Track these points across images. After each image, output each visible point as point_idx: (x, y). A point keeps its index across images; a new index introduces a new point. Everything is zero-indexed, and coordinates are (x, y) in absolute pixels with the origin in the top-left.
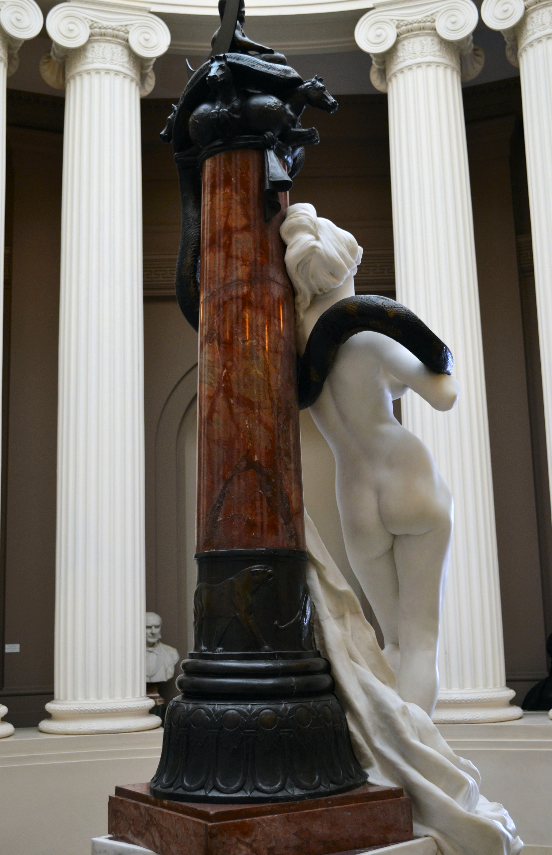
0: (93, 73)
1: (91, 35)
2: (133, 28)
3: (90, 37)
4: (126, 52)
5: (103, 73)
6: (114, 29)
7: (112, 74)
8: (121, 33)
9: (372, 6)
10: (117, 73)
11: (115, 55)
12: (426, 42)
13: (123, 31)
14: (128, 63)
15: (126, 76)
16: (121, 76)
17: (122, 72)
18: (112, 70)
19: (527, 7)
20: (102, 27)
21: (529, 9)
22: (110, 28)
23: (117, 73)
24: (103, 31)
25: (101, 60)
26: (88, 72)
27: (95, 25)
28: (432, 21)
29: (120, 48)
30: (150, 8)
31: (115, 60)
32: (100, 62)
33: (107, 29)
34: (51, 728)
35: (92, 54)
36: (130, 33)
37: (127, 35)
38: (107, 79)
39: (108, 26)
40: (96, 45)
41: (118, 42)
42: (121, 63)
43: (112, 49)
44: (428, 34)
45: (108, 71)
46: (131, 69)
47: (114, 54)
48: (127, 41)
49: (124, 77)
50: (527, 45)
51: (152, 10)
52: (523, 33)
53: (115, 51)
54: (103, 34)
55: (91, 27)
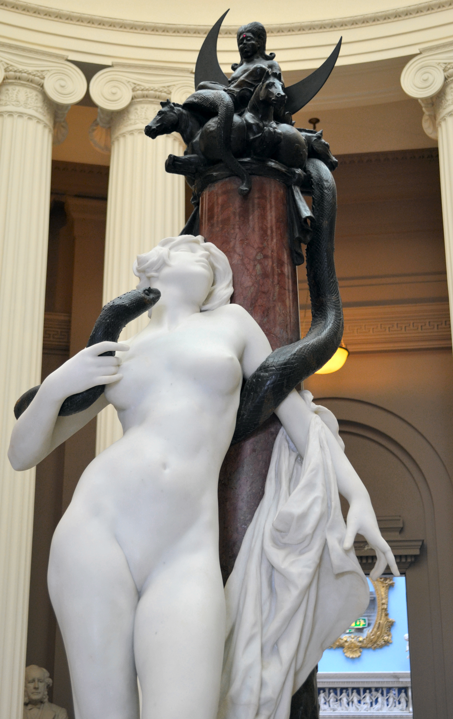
1: (6, 78)
2: (49, 74)
3: (4, 79)
4: (40, 97)
6: (29, 74)
7: (26, 118)
8: (37, 78)
10: (31, 117)
11: (30, 99)
14: (42, 108)
15: (39, 121)
16: (35, 121)
17: (35, 117)
18: (26, 114)
19: (447, 77)
20: (18, 71)
21: (449, 80)
22: (25, 72)
23: (31, 117)
24: (18, 74)
25: (14, 103)
29: (34, 93)
30: (68, 56)
31: (29, 104)
32: (13, 105)
33: (22, 73)
35: (6, 96)
36: (172, 94)
37: (42, 81)
38: (20, 122)
41: (33, 87)
42: (35, 108)
43: (26, 93)
45: (21, 115)
46: (45, 114)
47: (28, 98)
48: (42, 86)
49: (38, 122)
50: (446, 114)
51: (70, 58)
52: (442, 103)
53: (30, 95)
54: (18, 78)
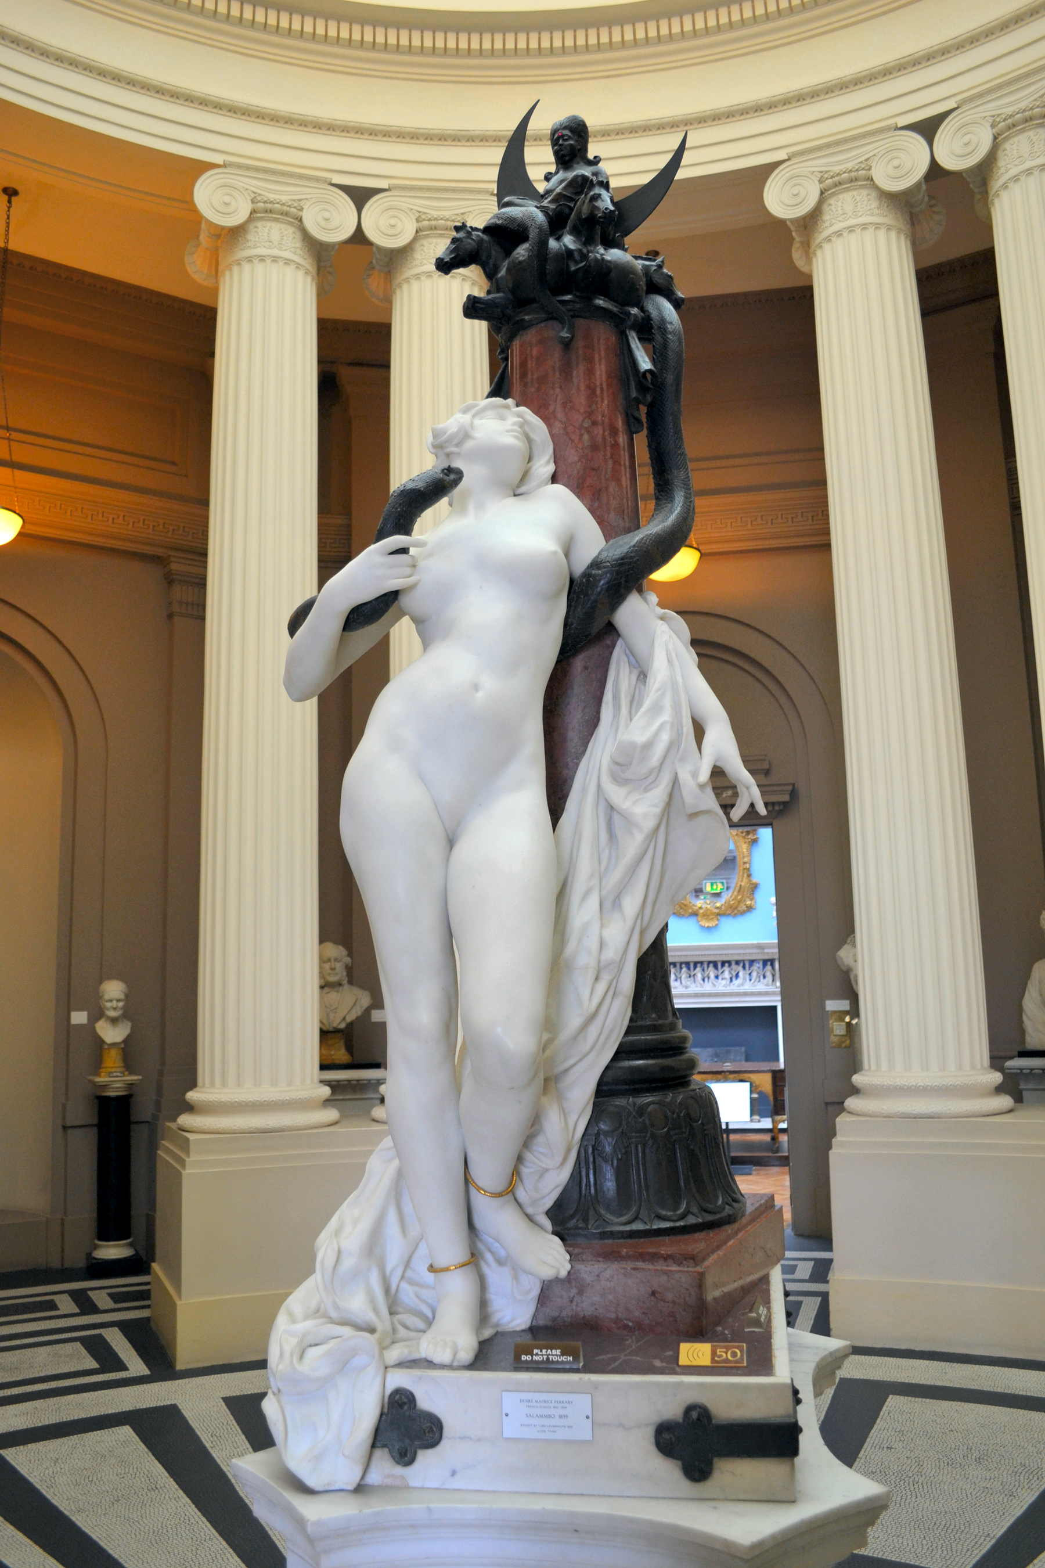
0: (256, 261)
2: (308, 204)
4: (298, 234)
5: (268, 261)
8: (293, 210)
10: (288, 262)
12: (860, 197)
13: (295, 207)
14: (301, 250)
15: (299, 266)
22: (278, 203)
23: (288, 262)
25: (266, 245)
28: (867, 168)
34: (195, 1125)
37: (300, 213)
38: (274, 269)
39: (275, 200)
41: (289, 221)
43: (281, 229)
44: (862, 187)
48: (301, 220)
49: (297, 267)
53: (285, 233)
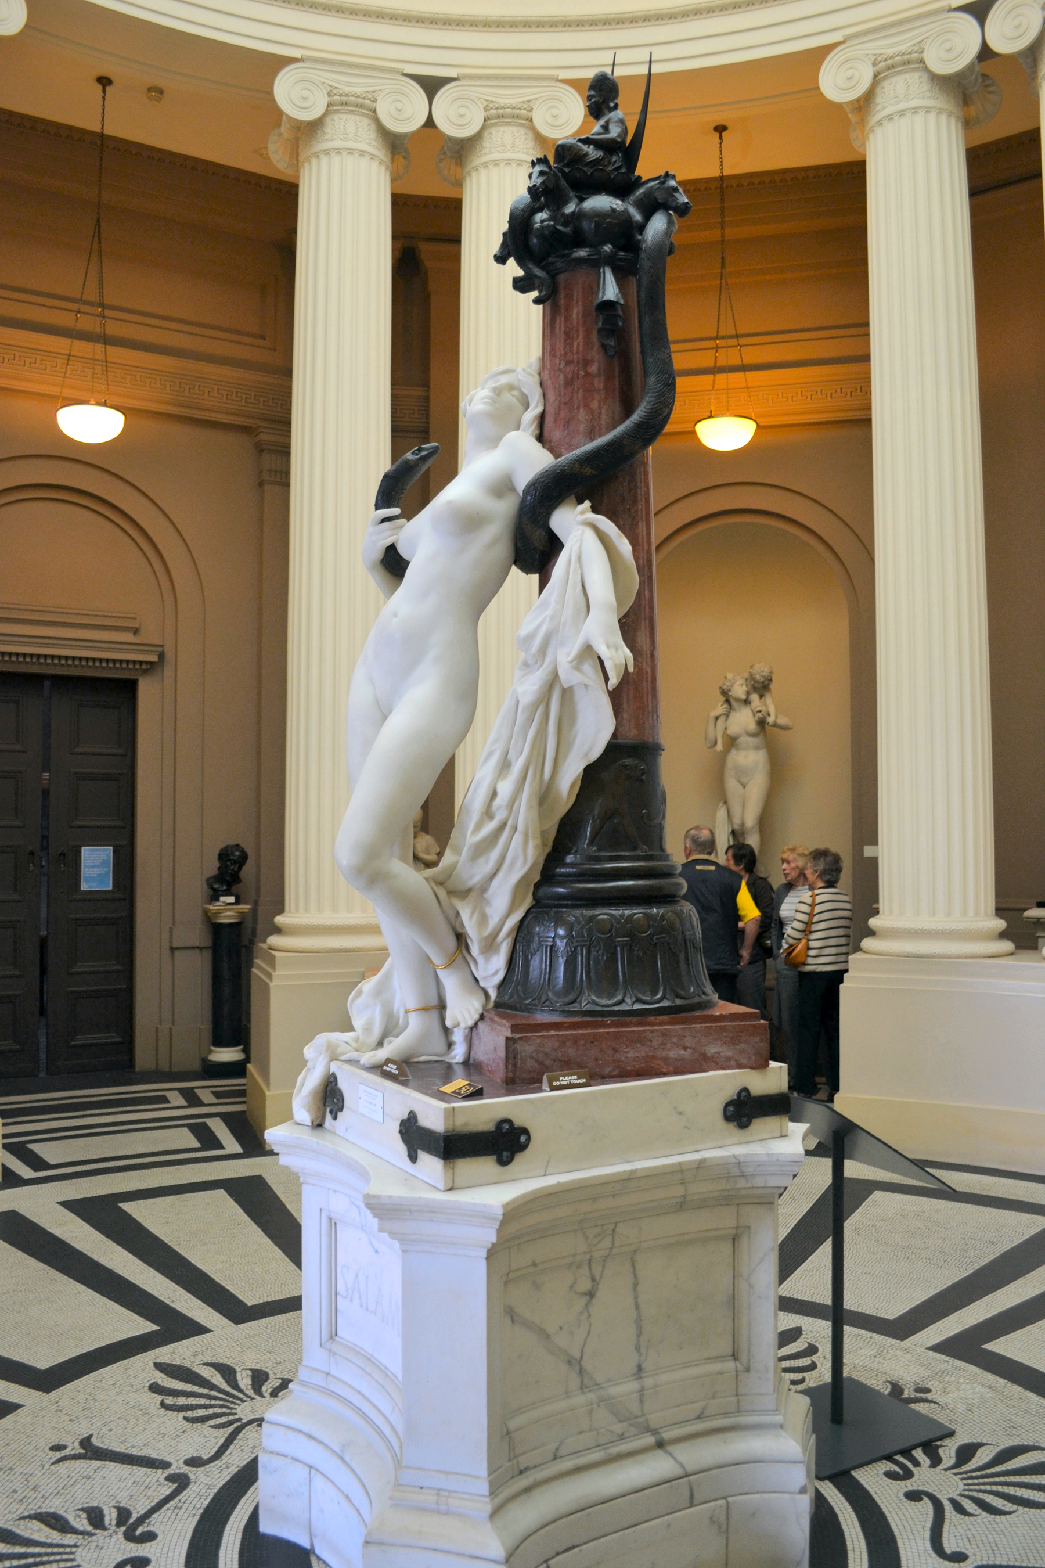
1: (330, 105)
3: (328, 106)
5: (344, 154)
6: (358, 97)
9: (841, 39)
10: (362, 153)
13: (369, 99)
15: (373, 157)
16: (367, 158)
23: (362, 153)
24: (344, 99)
26: (327, 152)
27: (335, 91)
40: (336, 117)
42: (367, 141)
45: (350, 151)
48: (375, 111)
55: (329, 95)
